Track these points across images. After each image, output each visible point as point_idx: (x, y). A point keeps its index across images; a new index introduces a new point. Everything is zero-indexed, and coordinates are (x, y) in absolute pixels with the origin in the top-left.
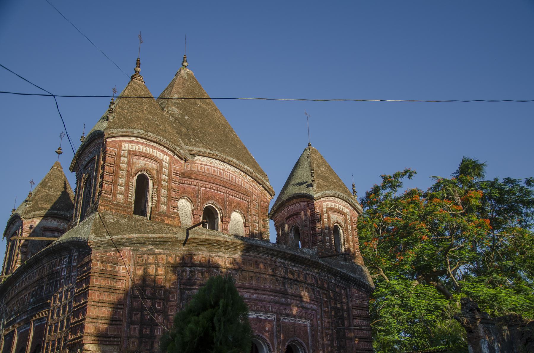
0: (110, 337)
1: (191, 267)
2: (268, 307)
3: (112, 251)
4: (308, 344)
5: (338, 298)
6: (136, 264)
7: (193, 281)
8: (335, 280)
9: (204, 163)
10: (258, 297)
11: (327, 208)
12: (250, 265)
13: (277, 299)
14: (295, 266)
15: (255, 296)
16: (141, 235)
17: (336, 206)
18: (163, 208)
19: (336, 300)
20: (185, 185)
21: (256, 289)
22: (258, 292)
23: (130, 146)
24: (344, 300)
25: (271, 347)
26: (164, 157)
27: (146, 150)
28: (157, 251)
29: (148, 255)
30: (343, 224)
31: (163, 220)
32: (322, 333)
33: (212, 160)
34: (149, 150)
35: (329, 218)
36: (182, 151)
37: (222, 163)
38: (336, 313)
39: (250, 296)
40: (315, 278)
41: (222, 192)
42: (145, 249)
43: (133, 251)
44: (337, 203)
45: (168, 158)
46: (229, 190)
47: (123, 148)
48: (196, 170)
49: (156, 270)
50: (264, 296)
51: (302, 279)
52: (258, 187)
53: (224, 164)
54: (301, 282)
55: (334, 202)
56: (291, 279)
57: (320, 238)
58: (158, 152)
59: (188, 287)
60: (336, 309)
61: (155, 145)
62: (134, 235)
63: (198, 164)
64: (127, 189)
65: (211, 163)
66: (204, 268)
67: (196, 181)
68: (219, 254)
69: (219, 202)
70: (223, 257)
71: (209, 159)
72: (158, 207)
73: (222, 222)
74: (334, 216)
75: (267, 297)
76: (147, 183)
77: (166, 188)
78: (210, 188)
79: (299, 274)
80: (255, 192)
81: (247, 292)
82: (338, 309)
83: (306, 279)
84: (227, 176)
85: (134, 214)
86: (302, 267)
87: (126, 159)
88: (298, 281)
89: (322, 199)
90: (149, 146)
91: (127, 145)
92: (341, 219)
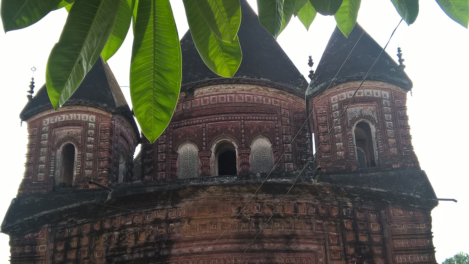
1: (119, 230)
5: (361, 227)
6: (56, 241)
7: (124, 245)
8: (353, 203)
10: (214, 249)
13: (245, 247)
14: (274, 198)
15: (210, 248)
16: (53, 210)
19: (355, 230)
21: (210, 239)
22: (214, 242)
24: (376, 228)
28: (79, 222)
38: (358, 251)
39: (202, 250)
40: (313, 206)
42: (65, 223)
43: (52, 227)
48: (198, 105)
49: (79, 242)
50: (223, 246)
51: (289, 212)
54: (286, 216)
56: (268, 217)
59: (117, 253)
60: (357, 244)
62: (46, 212)
63: (198, 98)
66: (136, 228)
68: (158, 207)
75: (229, 246)
81: (197, 246)
82: (361, 243)
83: (296, 210)
87: (47, 134)
88: (278, 216)
91: (48, 120)
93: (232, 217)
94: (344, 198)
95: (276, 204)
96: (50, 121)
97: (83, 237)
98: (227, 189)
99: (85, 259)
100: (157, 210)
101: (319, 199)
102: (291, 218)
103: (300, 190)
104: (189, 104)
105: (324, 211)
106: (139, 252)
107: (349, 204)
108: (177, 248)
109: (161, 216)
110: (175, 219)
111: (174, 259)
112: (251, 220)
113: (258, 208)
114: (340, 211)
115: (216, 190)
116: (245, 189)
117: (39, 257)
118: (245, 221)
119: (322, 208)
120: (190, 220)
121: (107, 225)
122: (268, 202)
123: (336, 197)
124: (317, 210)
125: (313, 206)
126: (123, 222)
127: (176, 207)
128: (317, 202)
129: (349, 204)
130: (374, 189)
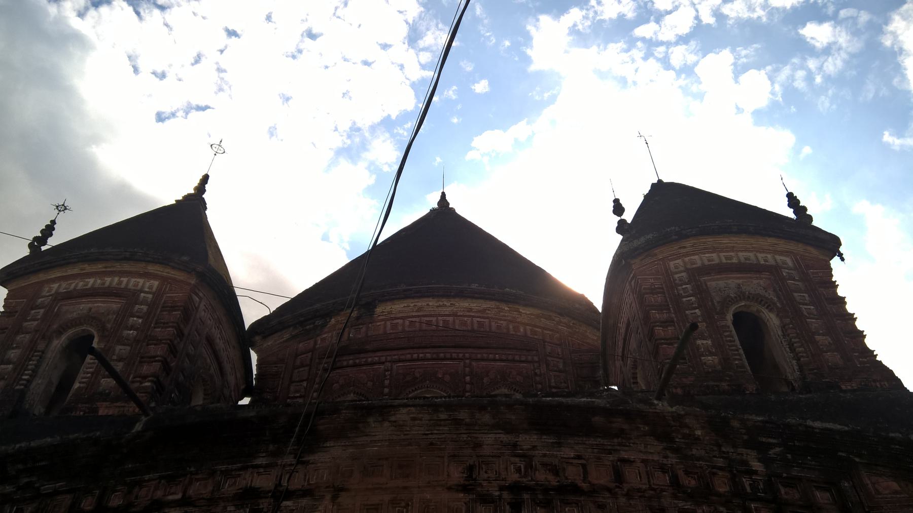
9: (401, 315)
11: (686, 270)
14: (559, 445)
20: (349, 369)
27: (104, 284)
30: (770, 295)
33: (421, 303)
36: (185, 258)
40: (663, 468)
41: (451, 359)
46: (470, 350)
51: (602, 482)
53: (453, 301)
61: (126, 267)
63: (382, 320)
67: (379, 354)
78: (418, 360)
79: (584, 466)
83: (619, 477)
86: (592, 441)
88: (575, 489)
90: (112, 274)
92: (755, 284)
93: (449, 489)
94: (740, 450)
98: (443, 416)
102: (608, 495)
103: (626, 427)
104: (364, 330)
105: (693, 482)
107: (757, 465)
109: (264, 482)
112: (500, 497)
113: (518, 470)
115: (414, 419)
116: (486, 418)
118: (485, 499)
119: (687, 473)
120: (337, 491)
122: (545, 455)
123: (719, 446)
124: (675, 482)
125: (663, 468)
126: (159, 494)
127: (306, 463)
128: (673, 460)
129: (757, 465)
130: (817, 424)
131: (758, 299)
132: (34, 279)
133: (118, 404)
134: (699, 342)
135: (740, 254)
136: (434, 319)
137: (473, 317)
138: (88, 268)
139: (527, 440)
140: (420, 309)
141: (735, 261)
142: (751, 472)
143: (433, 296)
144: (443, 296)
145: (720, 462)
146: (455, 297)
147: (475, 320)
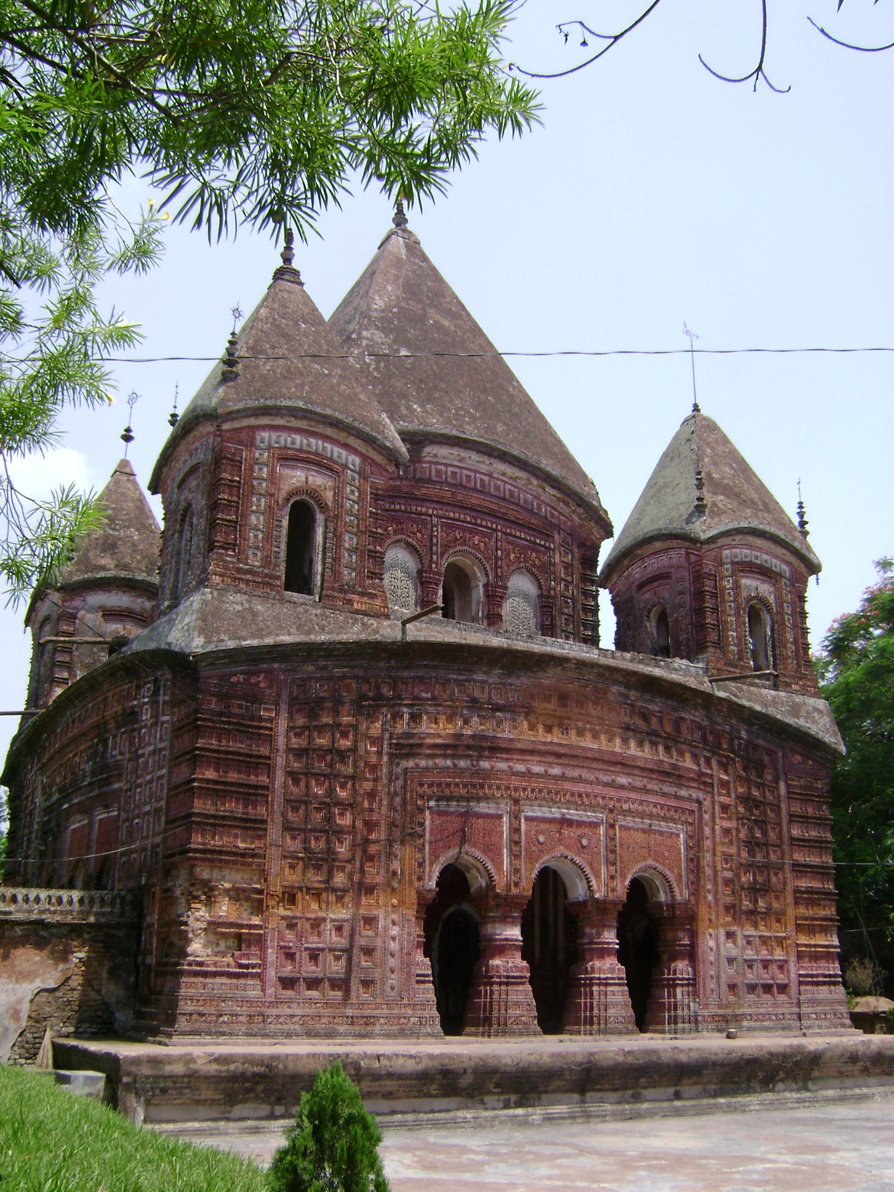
0: (243, 855)
2: (588, 796)
3: (242, 673)
4: (681, 876)
9: (444, 461)
11: (733, 563)
12: (547, 699)
15: (556, 771)
17: (757, 558)
18: (348, 575)
20: (400, 514)
21: (558, 755)
23: (274, 437)
25: (594, 883)
26: (350, 460)
29: (318, 680)
30: (772, 599)
31: (350, 602)
32: (714, 855)
33: (464, 454)
34: (316, 444)
35: (737, 587)
36: (388, 444)
37: (486, 460)
39: (546, 772)
42: (311, 668)
44: (759, 549)
45: (358, 460)
47: (258, 443)
51: (668, 730)
52: (574, 511)
53: (492, 461)
55: (750, 547)
57: (713, 636)
58: (336, 449)
61: (329, 431)
63: (430, 462)
64: (269, 537)
65: (460, 461)
68: (475, 677)
69: (479, 550)
70: (484, 682)
71: (455, 451)
72: (336, 574)
73: (487, 596)
74: (751, 584)
76: (313, 520)
77: (355, 530)
78: (459, 520)
79: (661, 718)
80: (565, 523)
83: (678, 730)
84: (497, 488)
85: (286, 590)
86: (669, 702)
88: (658, 735)
89: (721, 542)
90: (314, 434)
92: (765, 589)
95: (653, 713)
96: (270, 440)
97: (342, 703)
99: (349, 750)
100: (475, 681)
101: (708, 717)
106: (445, 756)
107: (744, 734)
108: (507, 760)
110: (504, 706)
111: (502, 779)
114: (731, 740)
117: (260, 728)
119: (711, 733)
121: (387, 692)
125: (700, 727)
128: (705, 723)
129: (744, 734)
131: (763, 601)
132: (246, 422)
133: (365, 599)
134: (730, 633)
135: (765, 557)
136: (473, 475)
137: (506, 482)
138: (295, 423)
139: (633, 694)
140: (461, 460)
141: (759, 562)
142: (740, 738)
143: (478, 451)
144: (486, 454)
145: (727, 728)
146: (495, 457)
147: (508, 487)
